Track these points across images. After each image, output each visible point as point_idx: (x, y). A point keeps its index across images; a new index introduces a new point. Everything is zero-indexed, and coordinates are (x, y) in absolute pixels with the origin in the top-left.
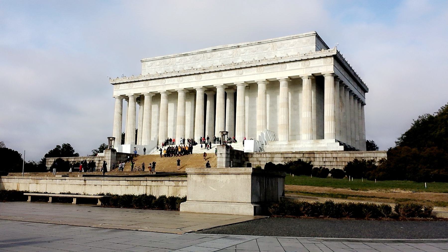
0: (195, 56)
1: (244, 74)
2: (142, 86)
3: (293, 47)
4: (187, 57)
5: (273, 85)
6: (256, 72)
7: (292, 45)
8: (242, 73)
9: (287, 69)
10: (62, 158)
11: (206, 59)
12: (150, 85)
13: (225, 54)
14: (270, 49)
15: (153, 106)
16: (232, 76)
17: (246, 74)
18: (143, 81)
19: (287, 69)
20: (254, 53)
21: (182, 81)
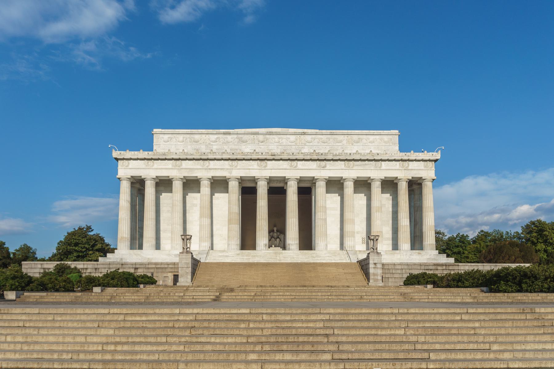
0: (240, 136)
1: (328, 167)
2: (170, 166)
3: (373, 144)
4: (229, 137)
5: (363, 185)
6: (343, 167)
7: (370, 142)
8: (325, 166)
9: (382, 168)
10: (69, 263)
11: (257, 142)
13: (284, 140)
14: (345, 142)
15: (217, 195)
16: (311, 167)
17: (331, 168)
18: (172, 159)
19: (382, 168)
21: (236, 167)
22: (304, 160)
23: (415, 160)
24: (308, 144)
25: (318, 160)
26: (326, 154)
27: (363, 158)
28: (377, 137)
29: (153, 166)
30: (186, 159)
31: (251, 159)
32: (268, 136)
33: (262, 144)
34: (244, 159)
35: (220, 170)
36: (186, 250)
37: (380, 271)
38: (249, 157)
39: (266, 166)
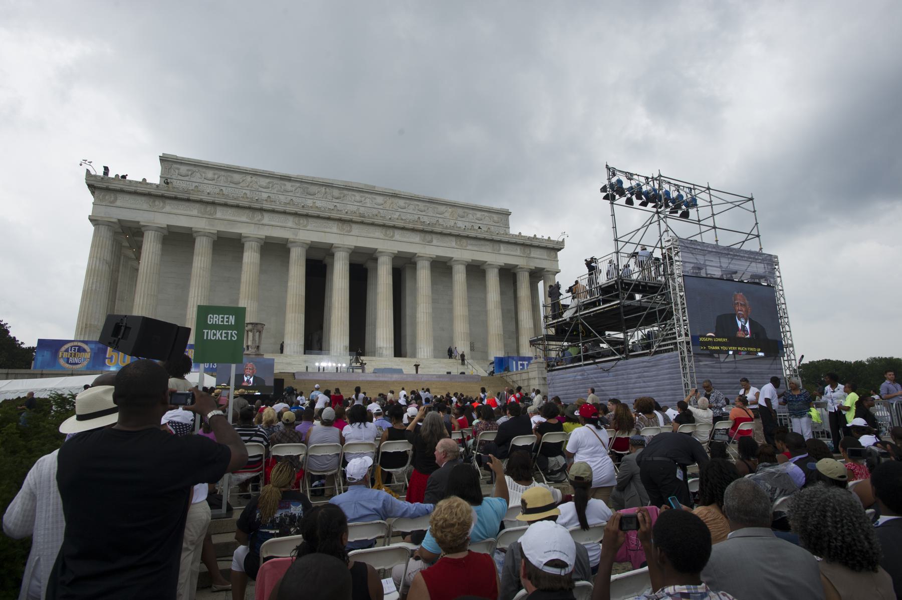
0: (306, 185)
1: (435, 242)
5: (476, 271)
6: (454, 244)
8: (432, 241)
11: (329, 197)
13: (368, 200)
16: (412, 240)
17: (438, 244)
21: (305, 226)
22: (403, 229)
25: (423, 231)
26: (434, 225)
28: (486, 214)
29: (163, 207)
30: (226, 205)
31: (329, 219)
32: (346, 192)
34: (318, 217)
38: (327, 214)
39: (350, 231)
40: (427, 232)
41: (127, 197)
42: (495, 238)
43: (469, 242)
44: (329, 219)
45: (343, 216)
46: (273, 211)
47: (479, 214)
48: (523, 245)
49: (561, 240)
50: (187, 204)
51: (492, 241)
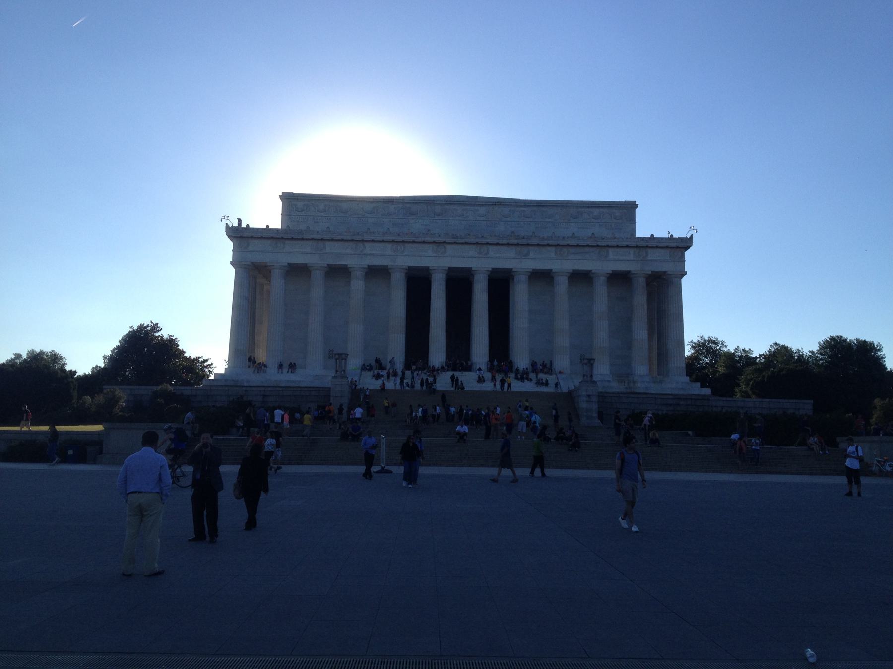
1: (532, 255)
6: (553, 255)
8: (528, 254)
12: (328, 250)
20: (528, 219)
23: (657, 247)
24: (504, 219)
25: (518, 245)
27: (581, 243)
28: (605, 210)
32: (447, 207)
33: (440, 217)
35: (378, 256)
36: (341, 373)
37: (595, 407)
40: (522, 245)
41: (257, 242)
42: (599, 243)
43: (571, 250)
44: (424, 242)
45: (436, 240)
46: (373, 241)
47: (596, 212)
48: (637, 247)
49: (688, 236)
50: (302, 242)
51: (598, 246)
